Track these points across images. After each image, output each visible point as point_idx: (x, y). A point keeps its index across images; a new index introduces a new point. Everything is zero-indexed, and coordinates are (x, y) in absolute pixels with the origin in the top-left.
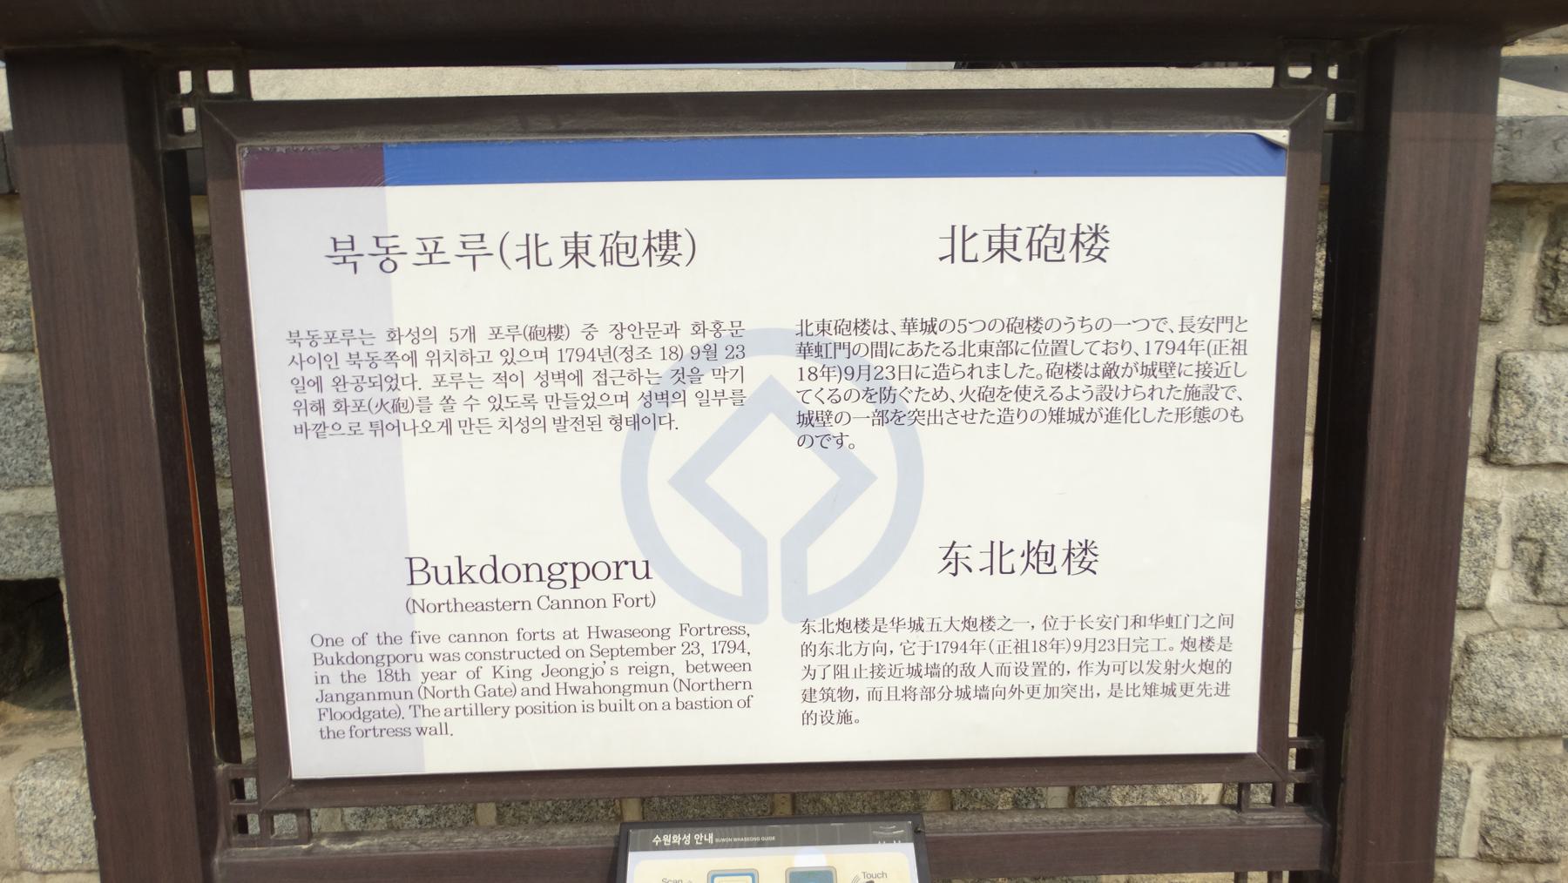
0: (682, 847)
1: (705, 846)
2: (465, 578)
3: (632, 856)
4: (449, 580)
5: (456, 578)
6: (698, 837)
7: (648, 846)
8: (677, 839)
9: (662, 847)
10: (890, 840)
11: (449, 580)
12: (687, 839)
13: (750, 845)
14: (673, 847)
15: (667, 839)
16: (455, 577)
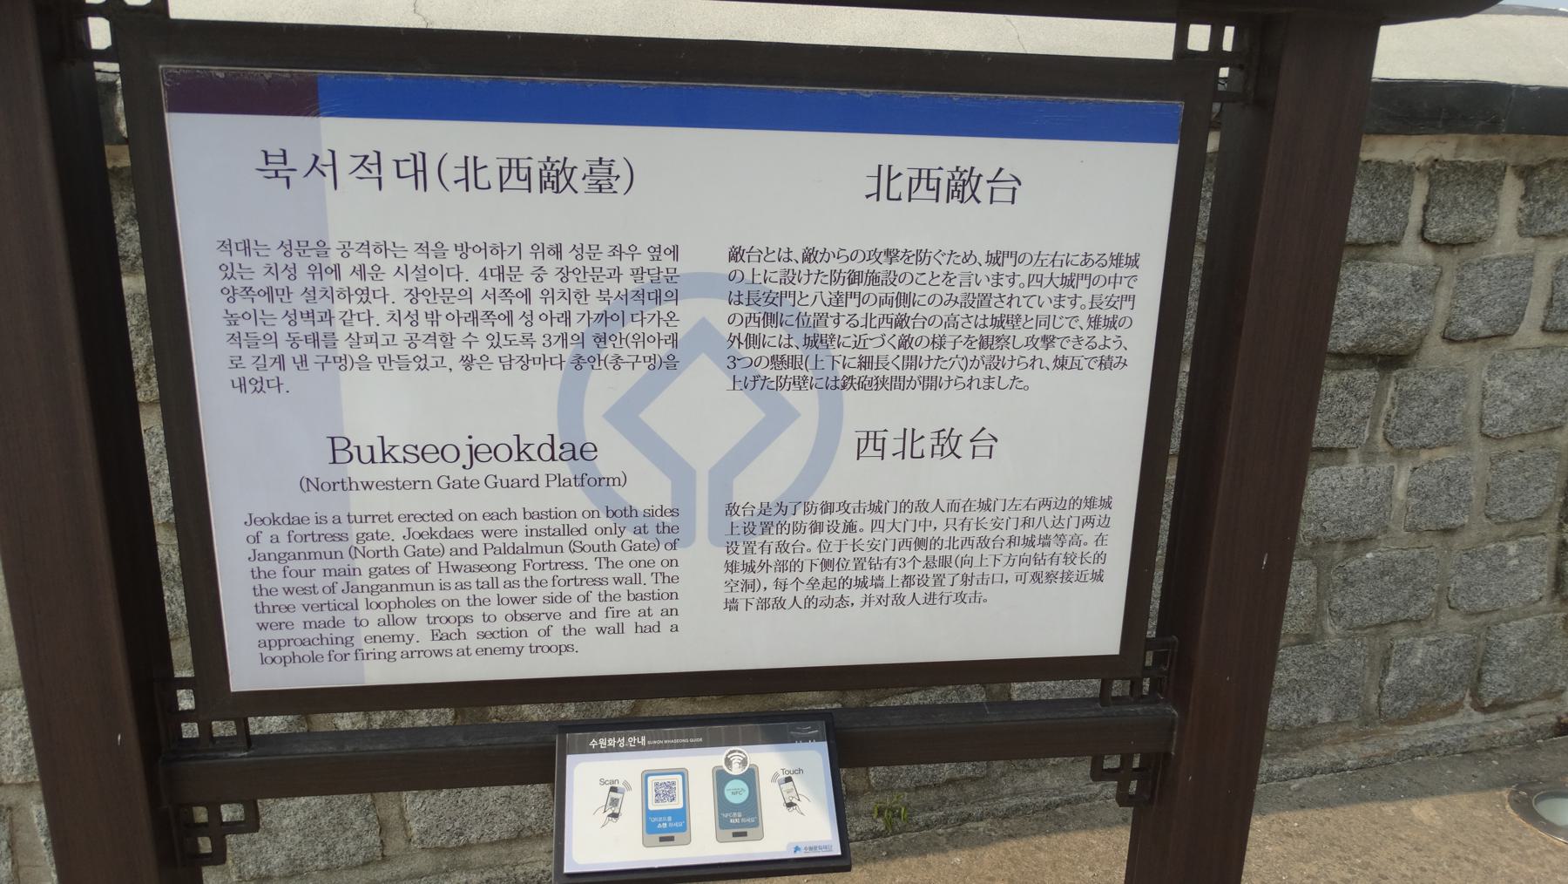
0: (617, 749)
1: (638, 748)
2: (388, 458)
3: (570, 758)
4: (372, 460)
5: (378, 457)
6: (632, 740)
7: (585, 749)
8: (612, 742)
9: (598, 750)
10: (805, 740)
11: (372, 460)
12: (621, 741)
13: (680, 746)
14: (609, 750)
15: (603, 742)
16: (378, 457)
